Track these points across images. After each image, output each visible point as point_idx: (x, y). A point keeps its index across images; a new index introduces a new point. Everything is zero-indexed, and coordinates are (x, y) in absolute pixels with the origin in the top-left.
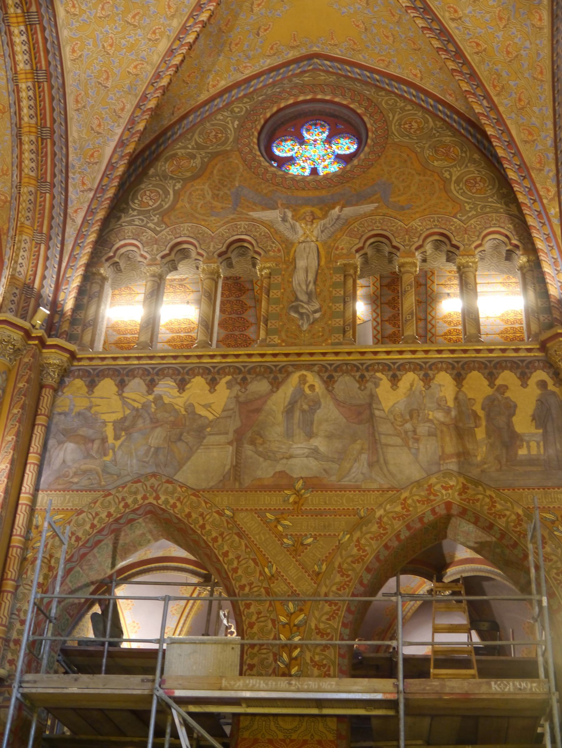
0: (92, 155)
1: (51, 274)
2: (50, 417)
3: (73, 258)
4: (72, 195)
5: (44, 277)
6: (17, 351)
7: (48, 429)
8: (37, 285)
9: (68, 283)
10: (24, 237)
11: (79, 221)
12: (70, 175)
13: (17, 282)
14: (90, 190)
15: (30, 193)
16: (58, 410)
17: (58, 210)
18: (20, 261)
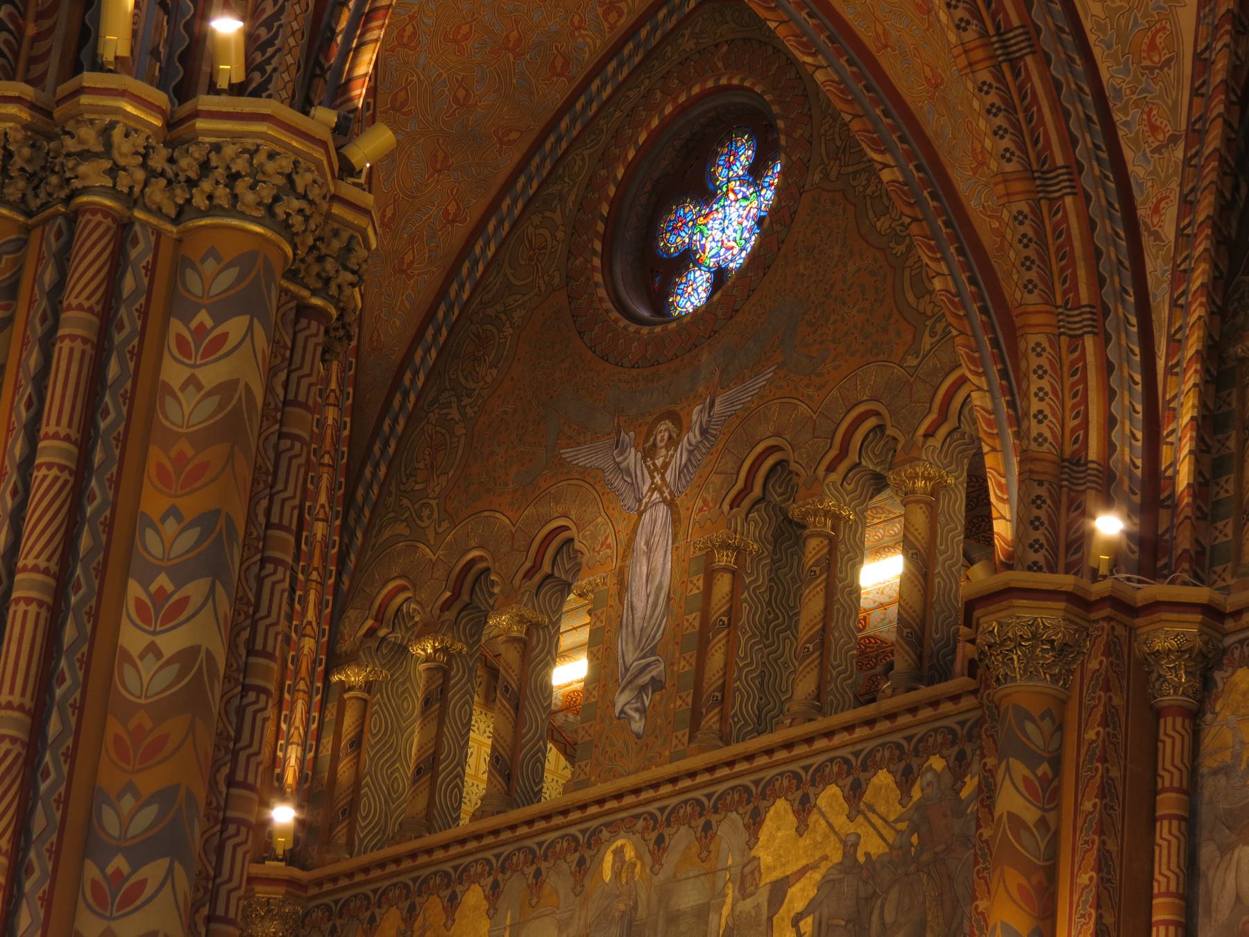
0: (1152, 46)
1: (1131, 403)
2: (1191, 789)
3: (1176, 344)
4: (1136, 169)
5: (1110, 422)
6: (1062, 650)
7: (1190, 823)
8: (1093, 453)
9: (1174, 415)
10: (1032, 340)
11: (1169, 232)
12: (1118, 117)
13: (1038, 467)
14: (1174, 139)
15: (1019, 218)
16: (1208, 763)
17: (1109, 229)
18: (1035, 406)
